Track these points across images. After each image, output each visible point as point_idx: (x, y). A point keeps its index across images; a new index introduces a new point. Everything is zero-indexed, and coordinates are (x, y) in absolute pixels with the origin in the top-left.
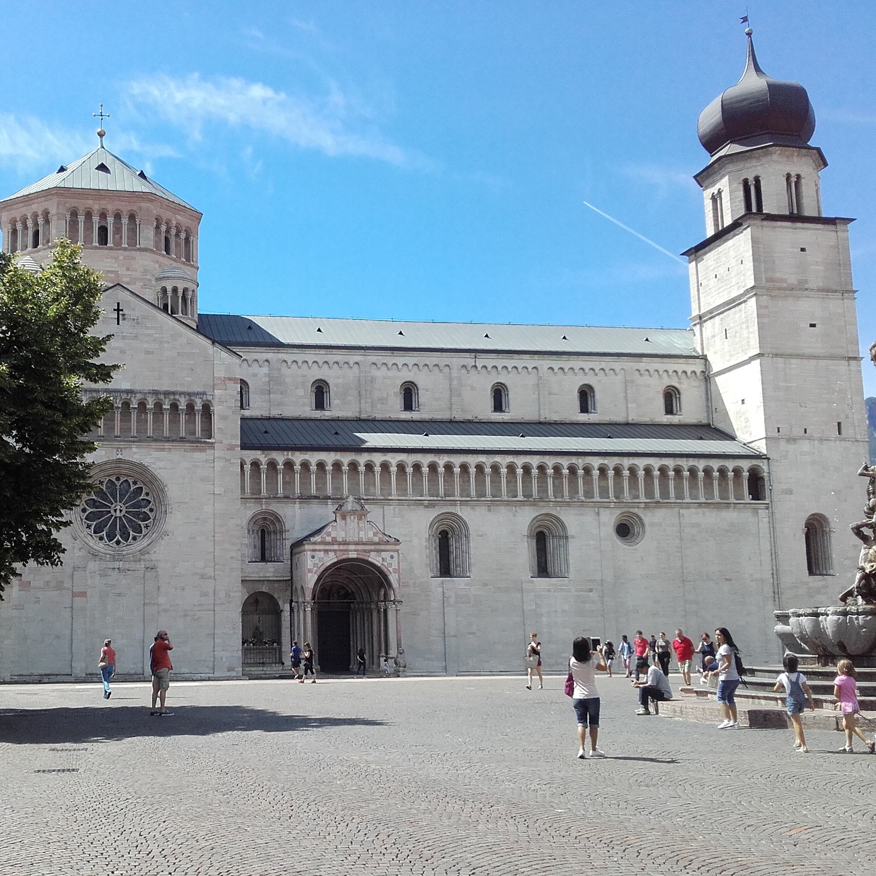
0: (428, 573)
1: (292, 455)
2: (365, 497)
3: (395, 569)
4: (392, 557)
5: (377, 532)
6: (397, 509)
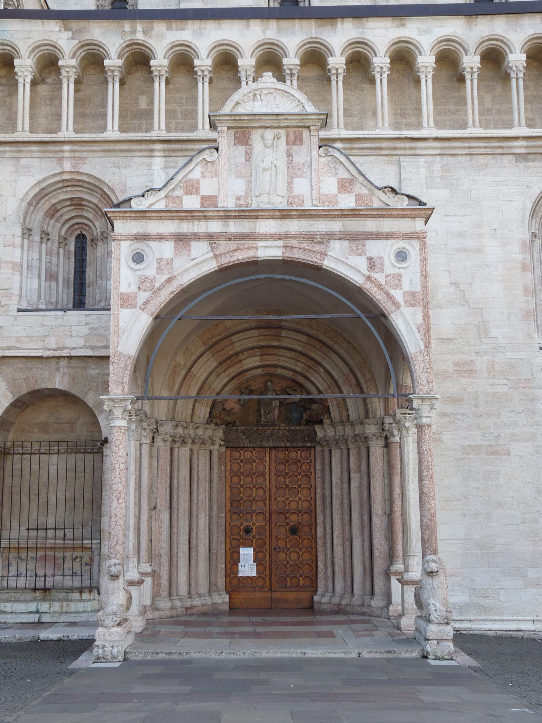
0: (529, 336)
1: (145, 33)
2: (345, 133)
3: (413, 294)
4: (402, 256)
5: (352, 181)
6: (437, 167)
